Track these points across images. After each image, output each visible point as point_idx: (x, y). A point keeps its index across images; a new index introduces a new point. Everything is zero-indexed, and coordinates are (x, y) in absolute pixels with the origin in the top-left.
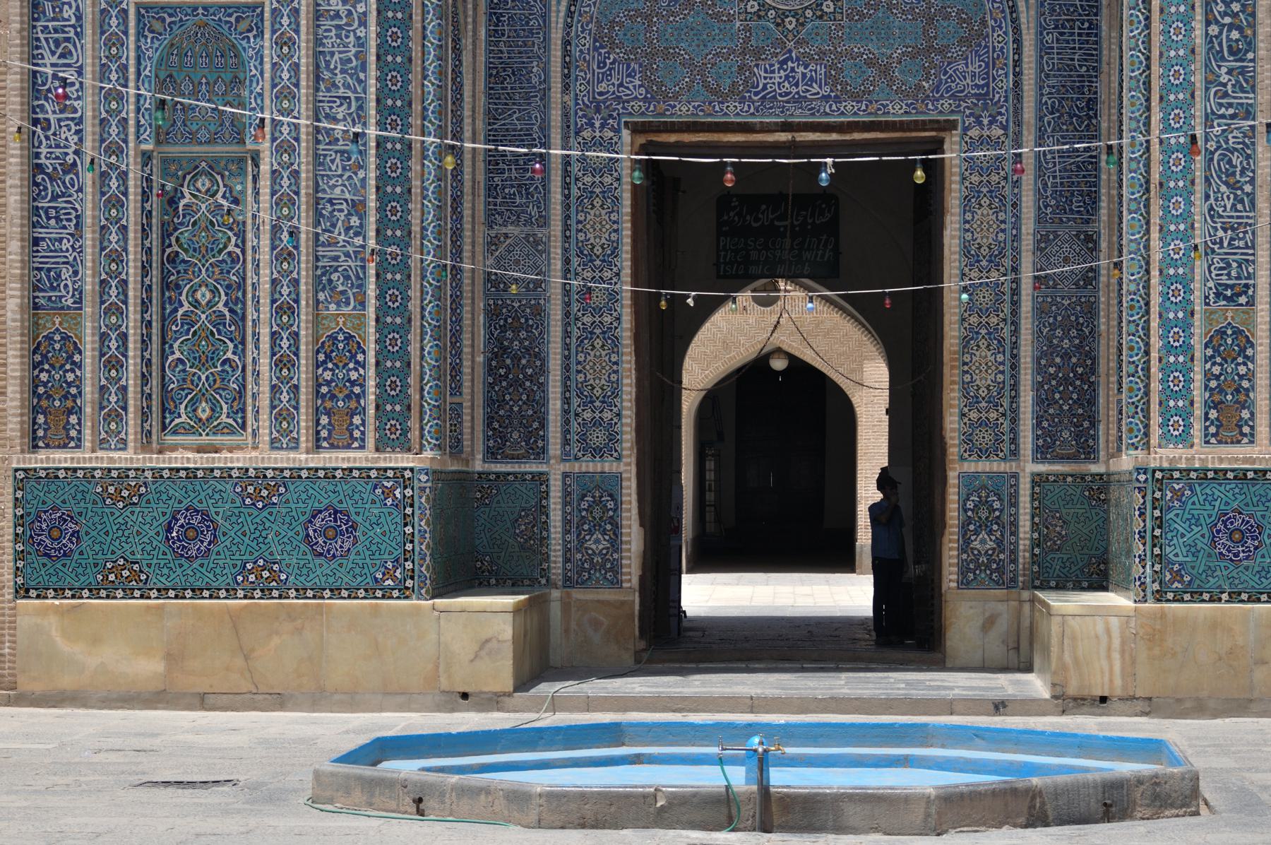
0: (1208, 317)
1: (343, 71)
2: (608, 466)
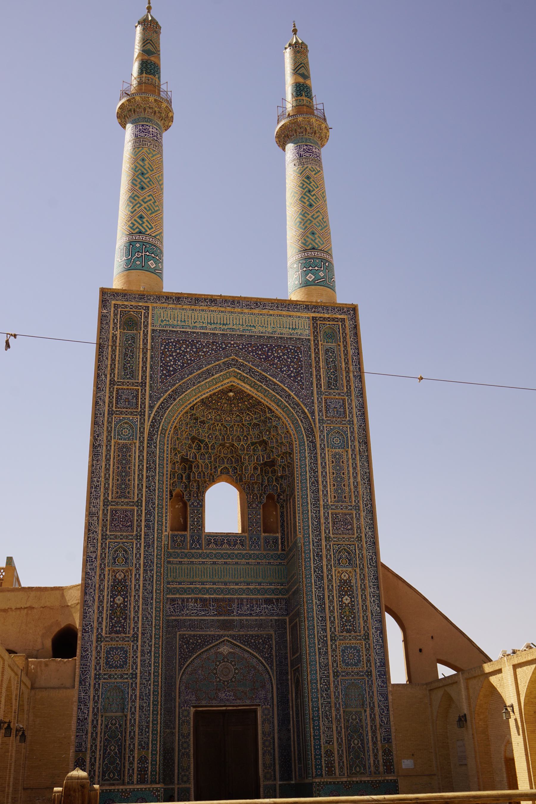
0: (325, 747)
2: (187, 785)
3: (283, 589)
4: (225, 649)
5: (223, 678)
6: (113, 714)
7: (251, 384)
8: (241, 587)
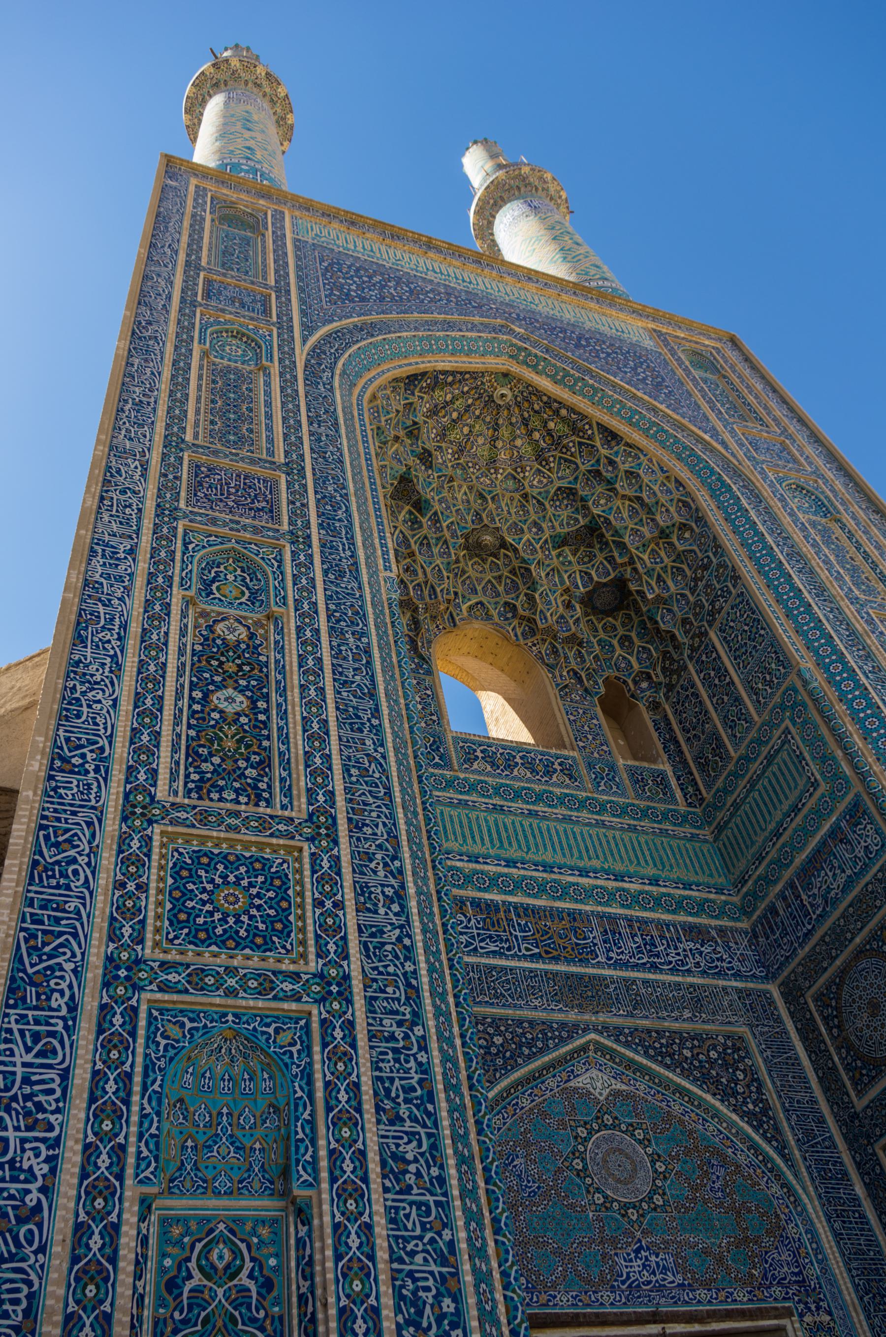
1: (406, 1101)
3: (726, 903)
4: (596, 1081)
5: (615, 1190)
6: (210, 1205)
7: (557, 374)
8: (599, 882)
